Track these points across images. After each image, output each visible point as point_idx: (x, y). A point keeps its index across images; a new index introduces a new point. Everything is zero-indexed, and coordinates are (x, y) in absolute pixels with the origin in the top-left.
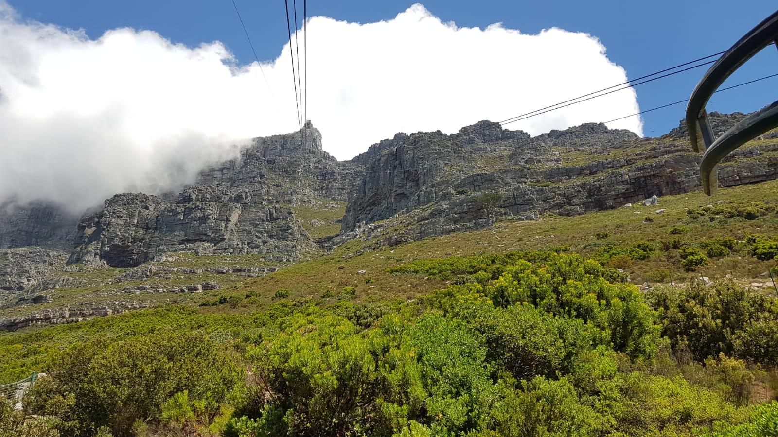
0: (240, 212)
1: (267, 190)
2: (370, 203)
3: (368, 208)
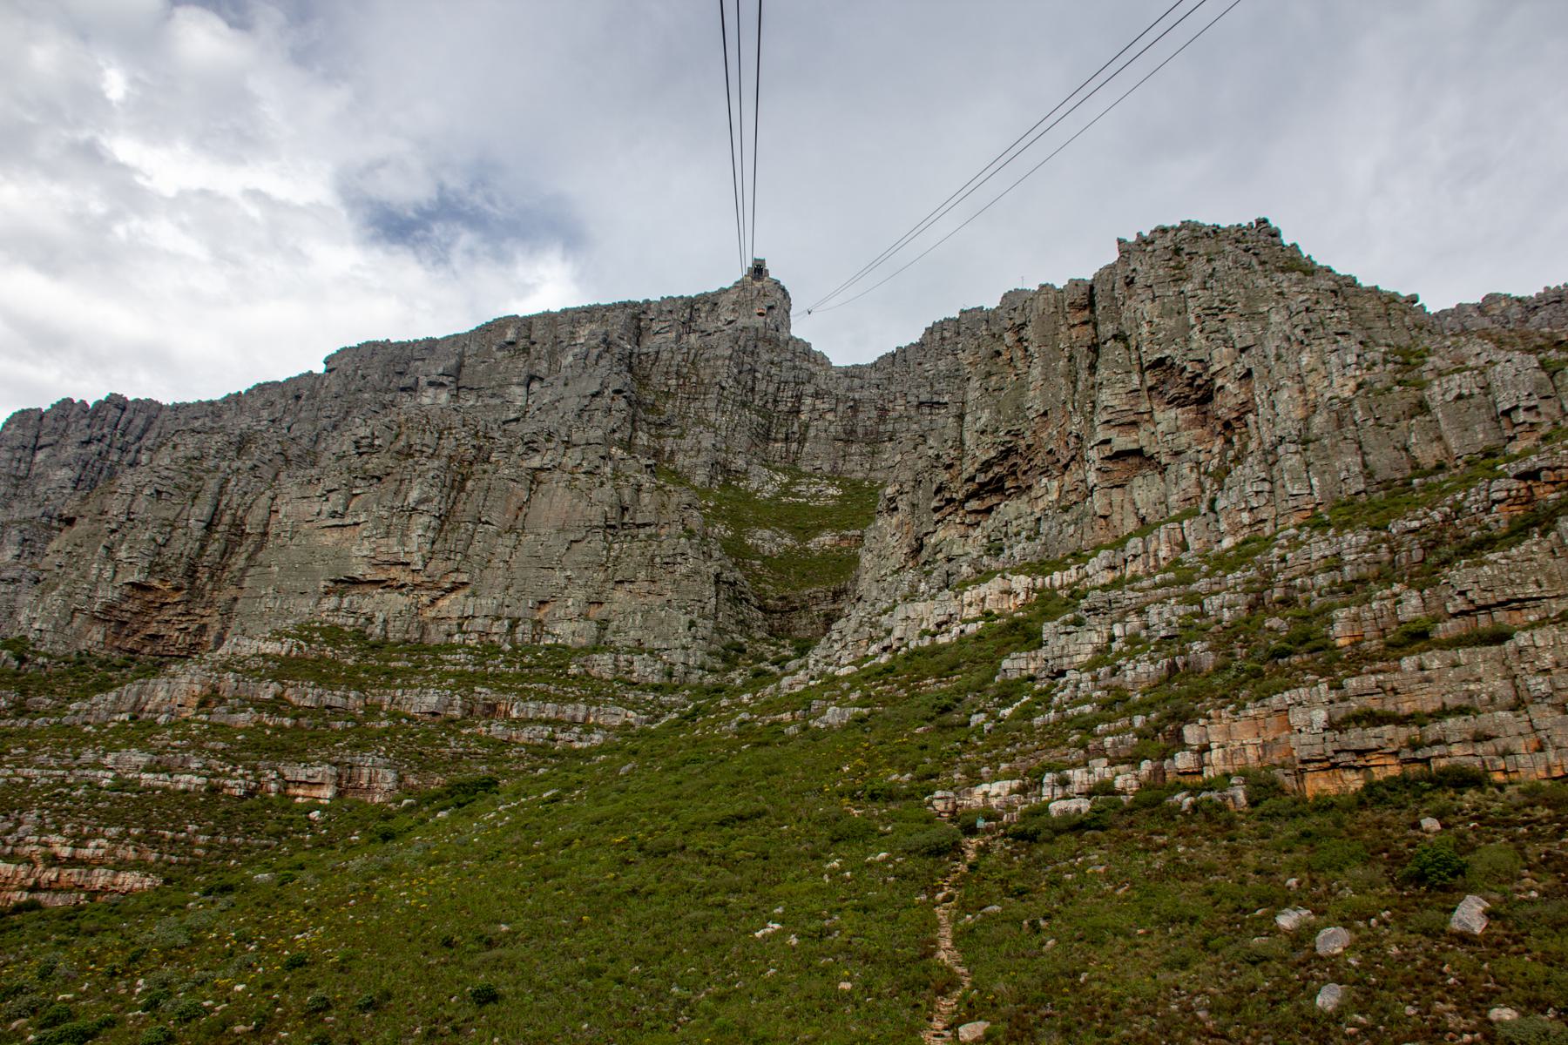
1: (627, 434)
2: (982, 485)
3: (973, 504)
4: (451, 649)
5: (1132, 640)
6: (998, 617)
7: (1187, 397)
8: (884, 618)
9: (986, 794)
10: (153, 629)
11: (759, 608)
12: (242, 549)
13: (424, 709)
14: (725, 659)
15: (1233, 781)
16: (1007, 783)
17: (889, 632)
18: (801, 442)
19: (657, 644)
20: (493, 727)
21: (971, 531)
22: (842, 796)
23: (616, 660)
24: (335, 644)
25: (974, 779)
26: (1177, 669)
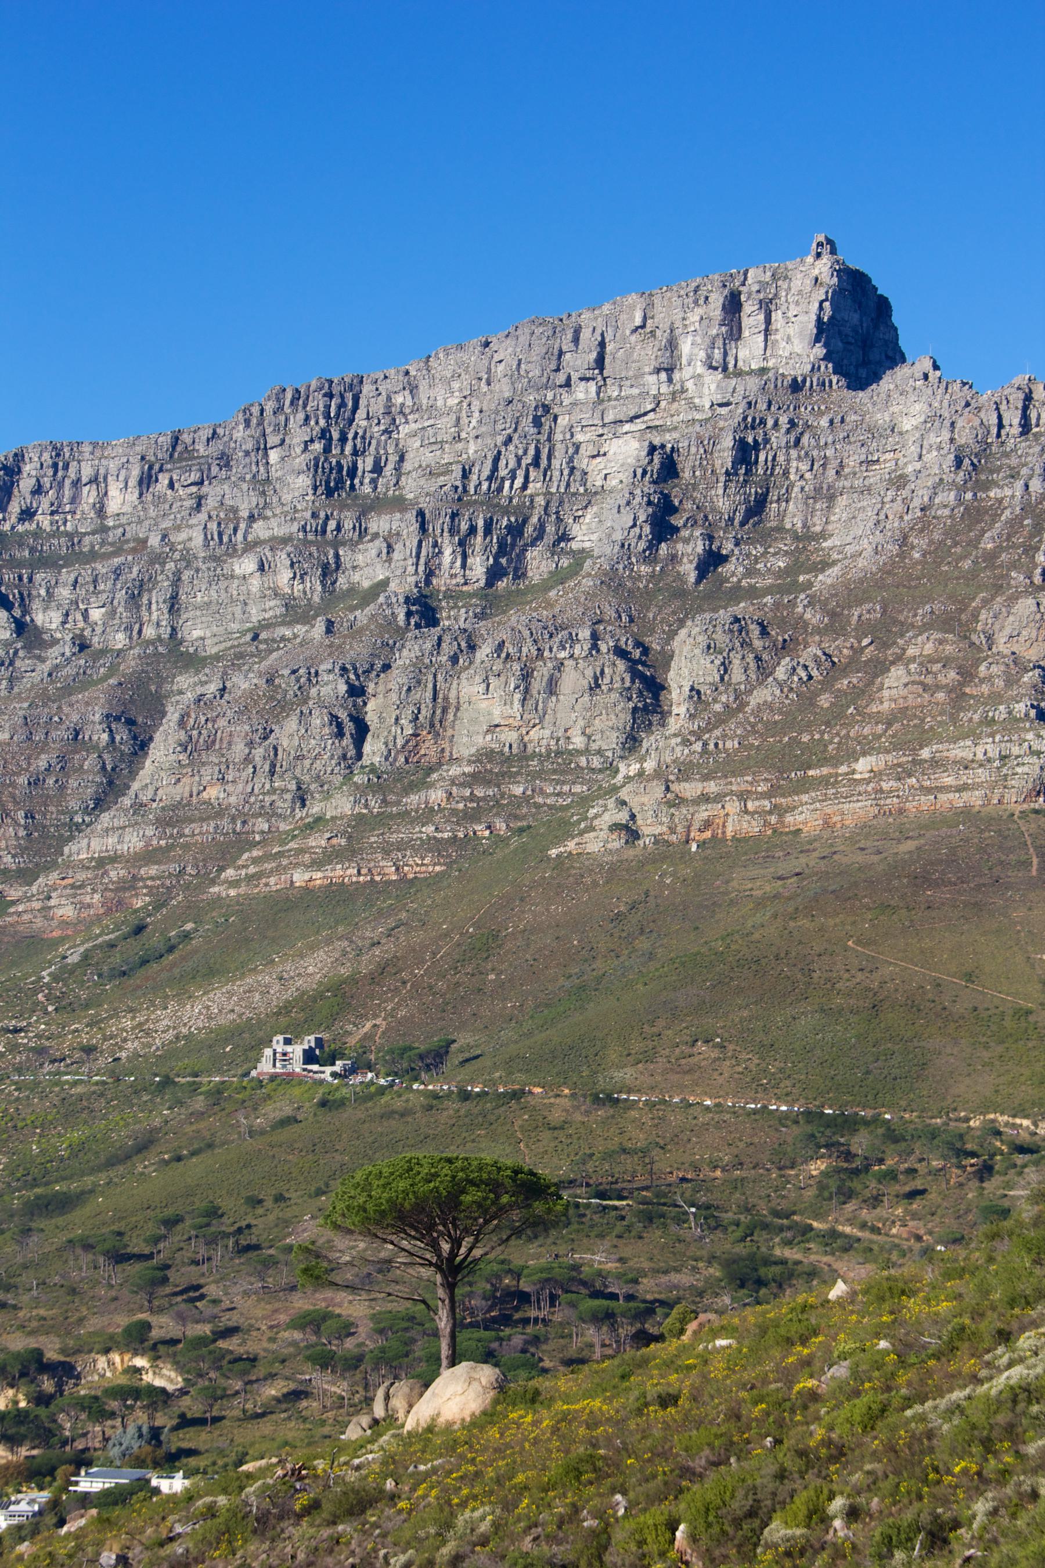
10: (422, 752)
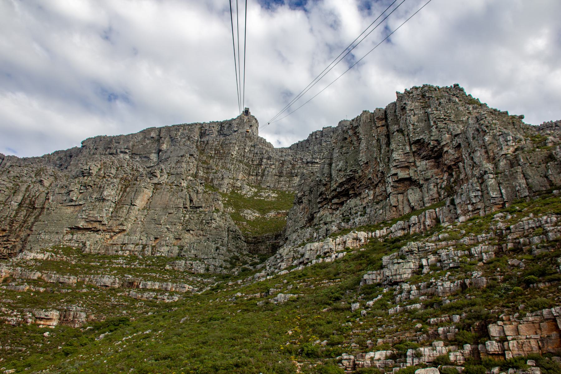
0: (150, 194)
1: (195, 172)
3: (335, 201)
4: (117, 257)
5: (433, 267)
6: (352, 250)
7: (430, 156)
8: (300, 249)
9: (372, 359)
11: (245, 242)
12: (33, 214)
13: (102, 284)
14: (231, 263)
15: (529, 363)
16: (384, 352)
17: (303, 255)
18: (262, 177)
19: (203, 256)
20: (131, 292)
21: (334, 212)
22: (290, 353)
23: (186, 263)
24: (68, 255)
25: (365, 349)
26: (466, 286)
